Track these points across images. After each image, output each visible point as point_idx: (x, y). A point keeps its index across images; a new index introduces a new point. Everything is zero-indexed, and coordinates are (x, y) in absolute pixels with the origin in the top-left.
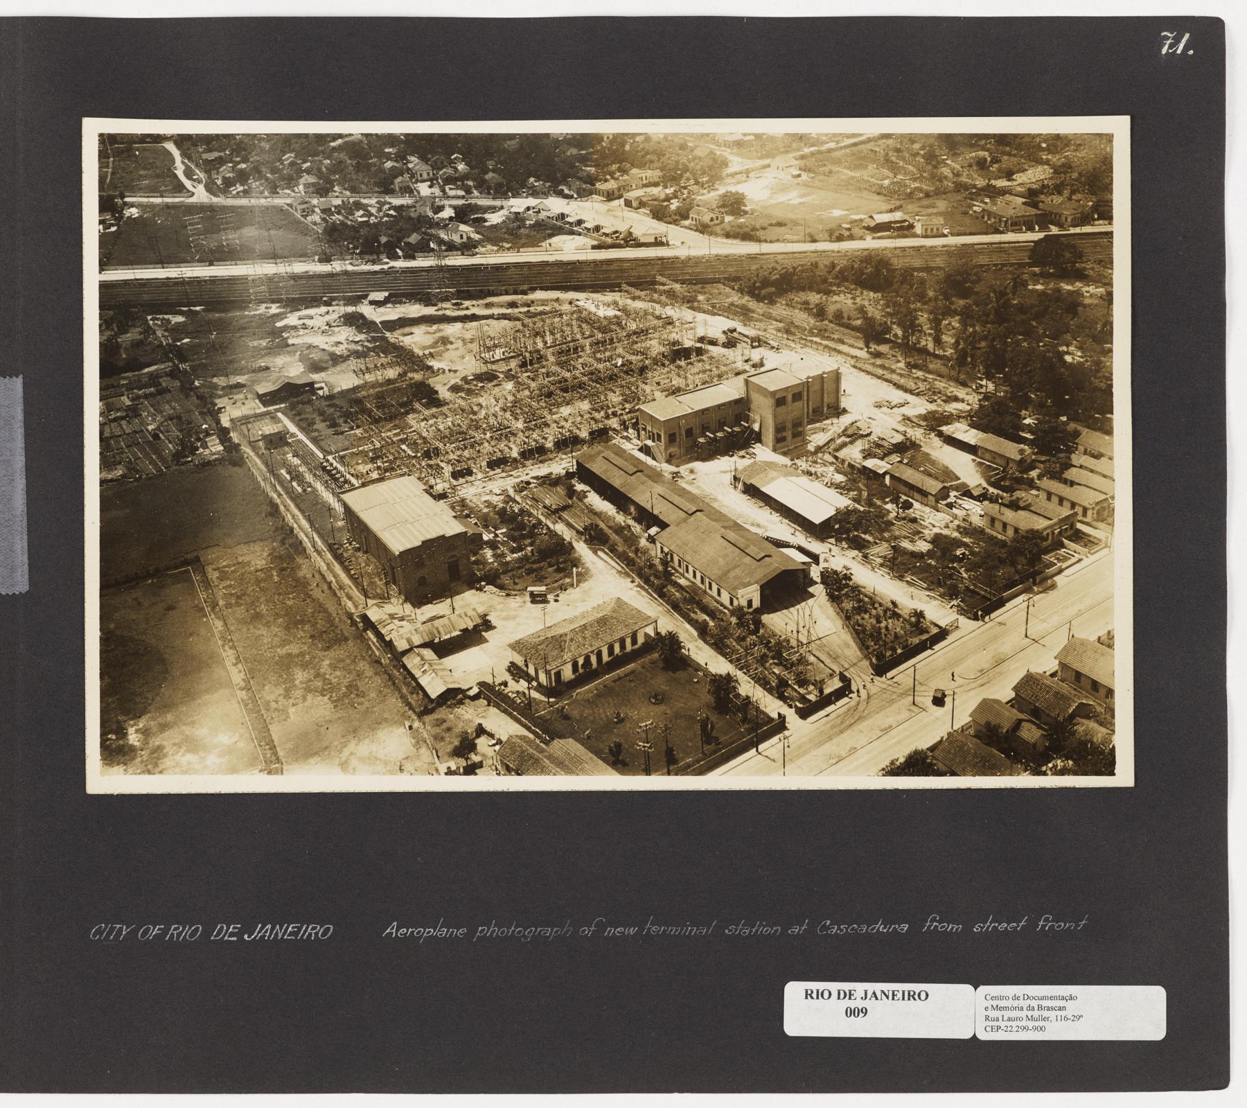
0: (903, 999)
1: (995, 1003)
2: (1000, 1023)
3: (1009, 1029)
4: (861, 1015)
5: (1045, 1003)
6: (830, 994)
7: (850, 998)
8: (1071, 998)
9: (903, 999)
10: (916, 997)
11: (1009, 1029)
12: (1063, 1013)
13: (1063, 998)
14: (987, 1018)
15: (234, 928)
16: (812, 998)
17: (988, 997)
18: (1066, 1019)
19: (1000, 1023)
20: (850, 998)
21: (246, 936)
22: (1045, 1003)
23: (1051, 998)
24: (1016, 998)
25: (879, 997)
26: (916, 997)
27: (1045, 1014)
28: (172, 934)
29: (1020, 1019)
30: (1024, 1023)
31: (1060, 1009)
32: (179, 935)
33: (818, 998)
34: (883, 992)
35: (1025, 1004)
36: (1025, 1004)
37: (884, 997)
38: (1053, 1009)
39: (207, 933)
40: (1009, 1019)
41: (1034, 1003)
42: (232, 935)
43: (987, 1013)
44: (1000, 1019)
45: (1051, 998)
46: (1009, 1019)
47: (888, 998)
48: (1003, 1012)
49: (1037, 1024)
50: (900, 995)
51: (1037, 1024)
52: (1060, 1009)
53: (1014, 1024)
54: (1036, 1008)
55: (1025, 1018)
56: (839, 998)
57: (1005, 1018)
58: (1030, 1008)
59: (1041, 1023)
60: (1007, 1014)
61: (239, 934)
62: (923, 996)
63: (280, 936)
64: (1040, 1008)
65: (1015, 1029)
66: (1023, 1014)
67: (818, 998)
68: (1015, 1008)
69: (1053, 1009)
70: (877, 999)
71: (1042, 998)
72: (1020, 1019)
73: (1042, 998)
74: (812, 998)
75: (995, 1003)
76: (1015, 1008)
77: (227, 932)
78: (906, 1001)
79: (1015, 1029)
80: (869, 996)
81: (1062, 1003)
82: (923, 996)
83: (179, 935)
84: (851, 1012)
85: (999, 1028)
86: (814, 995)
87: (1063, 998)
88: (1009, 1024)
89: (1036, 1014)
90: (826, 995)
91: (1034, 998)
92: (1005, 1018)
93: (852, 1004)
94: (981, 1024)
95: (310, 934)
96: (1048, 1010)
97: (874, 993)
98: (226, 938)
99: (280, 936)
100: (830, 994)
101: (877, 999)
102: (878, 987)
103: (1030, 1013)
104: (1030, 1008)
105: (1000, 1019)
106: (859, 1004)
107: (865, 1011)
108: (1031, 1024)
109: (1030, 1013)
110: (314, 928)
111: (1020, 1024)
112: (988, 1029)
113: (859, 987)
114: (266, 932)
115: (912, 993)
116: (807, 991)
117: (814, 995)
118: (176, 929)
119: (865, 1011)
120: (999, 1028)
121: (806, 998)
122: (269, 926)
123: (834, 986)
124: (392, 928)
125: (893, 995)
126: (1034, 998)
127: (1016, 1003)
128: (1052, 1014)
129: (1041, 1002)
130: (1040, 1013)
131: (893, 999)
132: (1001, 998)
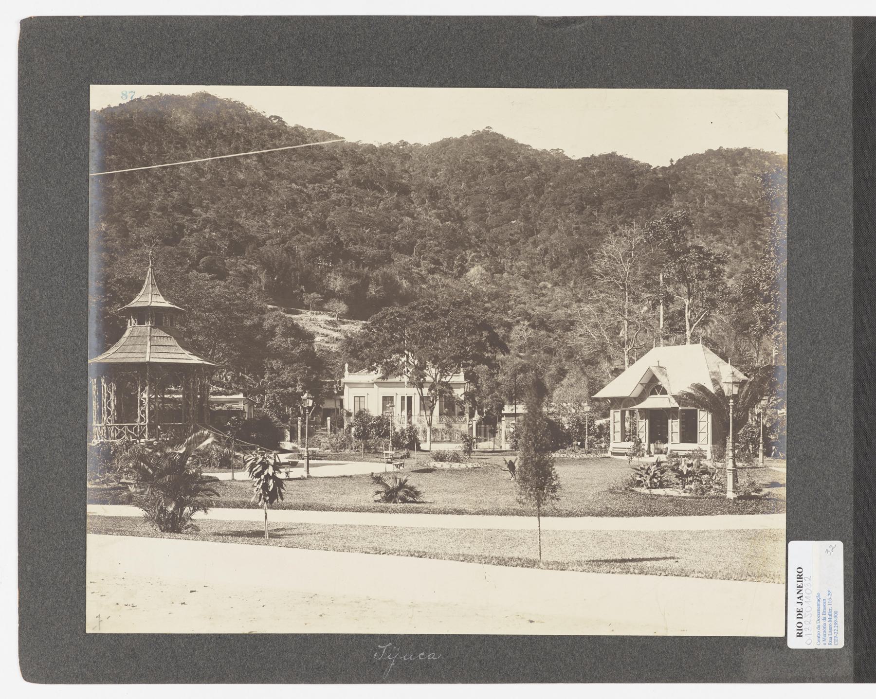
1: (822, 639)
2: (833, 637)
5: (822, 612)
8: (819, 596)
11: (836, 631)
12: (827, 601)
13: (819, 600)
14: (830, 644)
18: (830, 599)
19: (833, 637)
23: (819, 609)
24: (819, 628)
27: (827, 611)
29: (830, 625)
31: (824, 602)
35: (822, 622)
38: (825, 606)
40: (831, 631)
41: (822, 617)
44: (830, 636)
45: (819, 609)
46: (831, 631)
49: (833, 616)
51: (833, 616)
52: (824, 602)
55: (830, 622)
65: (836, 628)
66: (828, 624)
69: (825, 609)
72: (830, 625)
73: (819, 612)
75: (822, 639)
79: (836, 628)
85: (835, 637)
87: (819, 600)
88: (833, 632)
89: (827, 616)
96: (825, 609)
105: (831, 636)
108: (833, 619)
111: (833, 626)
120: (835, 637)
127: (822, 628)
128: (828, 607)
130: (827, 614)
132: (819, 636)
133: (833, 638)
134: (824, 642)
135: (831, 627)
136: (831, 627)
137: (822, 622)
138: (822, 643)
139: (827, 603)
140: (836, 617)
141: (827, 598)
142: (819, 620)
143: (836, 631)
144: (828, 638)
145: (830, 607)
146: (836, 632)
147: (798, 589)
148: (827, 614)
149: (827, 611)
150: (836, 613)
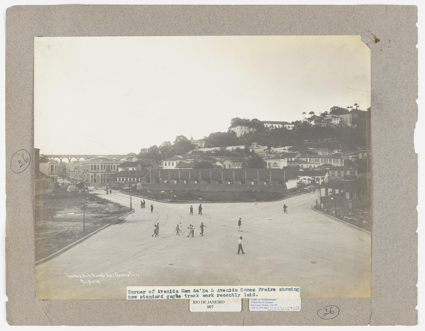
2: (255, 306)
3: (257, 308)
8: (275, 300)
12: (272, 304)
13: (272, 300)
14: (251, 305)
18: (273, 305)
19: (255, 306)
23: (269, 300)
24: (259, 300)
27: (267, 304)
30: (261, 306)
31: (271, 303)
35: (262, 301)
38: (269, 303)
40: (257, 305)
41: (264, 301)
43: (251, 304)
44: (255, 305)
45: (269, 300)
46: (257, 305)
49: (264, 306)
52: (271, 303)
53: (259, 307)
54: (265, 303)
55: (262, 305)
57: (256, 305)
58: (263, 302)
60: (257, 304)
64: (266, 302)
65: (259, 308)
66: (261, 304)
68: (259, 302)
69: (269, 303)
71: (267, 300)
73: (267, 300)
75: (254, 301)
76: (259, 302)
79: (259, 308)
85: (255, 308)
87: (272, 300)
88: (258, 306)
89: (265, 304)
92: (256, 305)
96: (268, 303)
103: (264, 304)
104: (263, 302)
105: (255, 305)
108: (263, 307)
109: (263, 304)
111: (260, 306)
112: (252, 308)
120: (255, 308)
127: (259, 301)
129: (266, 301)
130: (266, 304)
133: (254, 306)
135: (259, 305)
136: (259, 305)
137: (262, 301)
138: (252, 301)
139: (271, 304)
140: (264, 308)
141: (274, 304)
143: (257, 308)
144: (254, 304)
145: (269, 305)
146: (257, 308)
147: (215, 301)
148: (266, 304)
150: (266, 308)
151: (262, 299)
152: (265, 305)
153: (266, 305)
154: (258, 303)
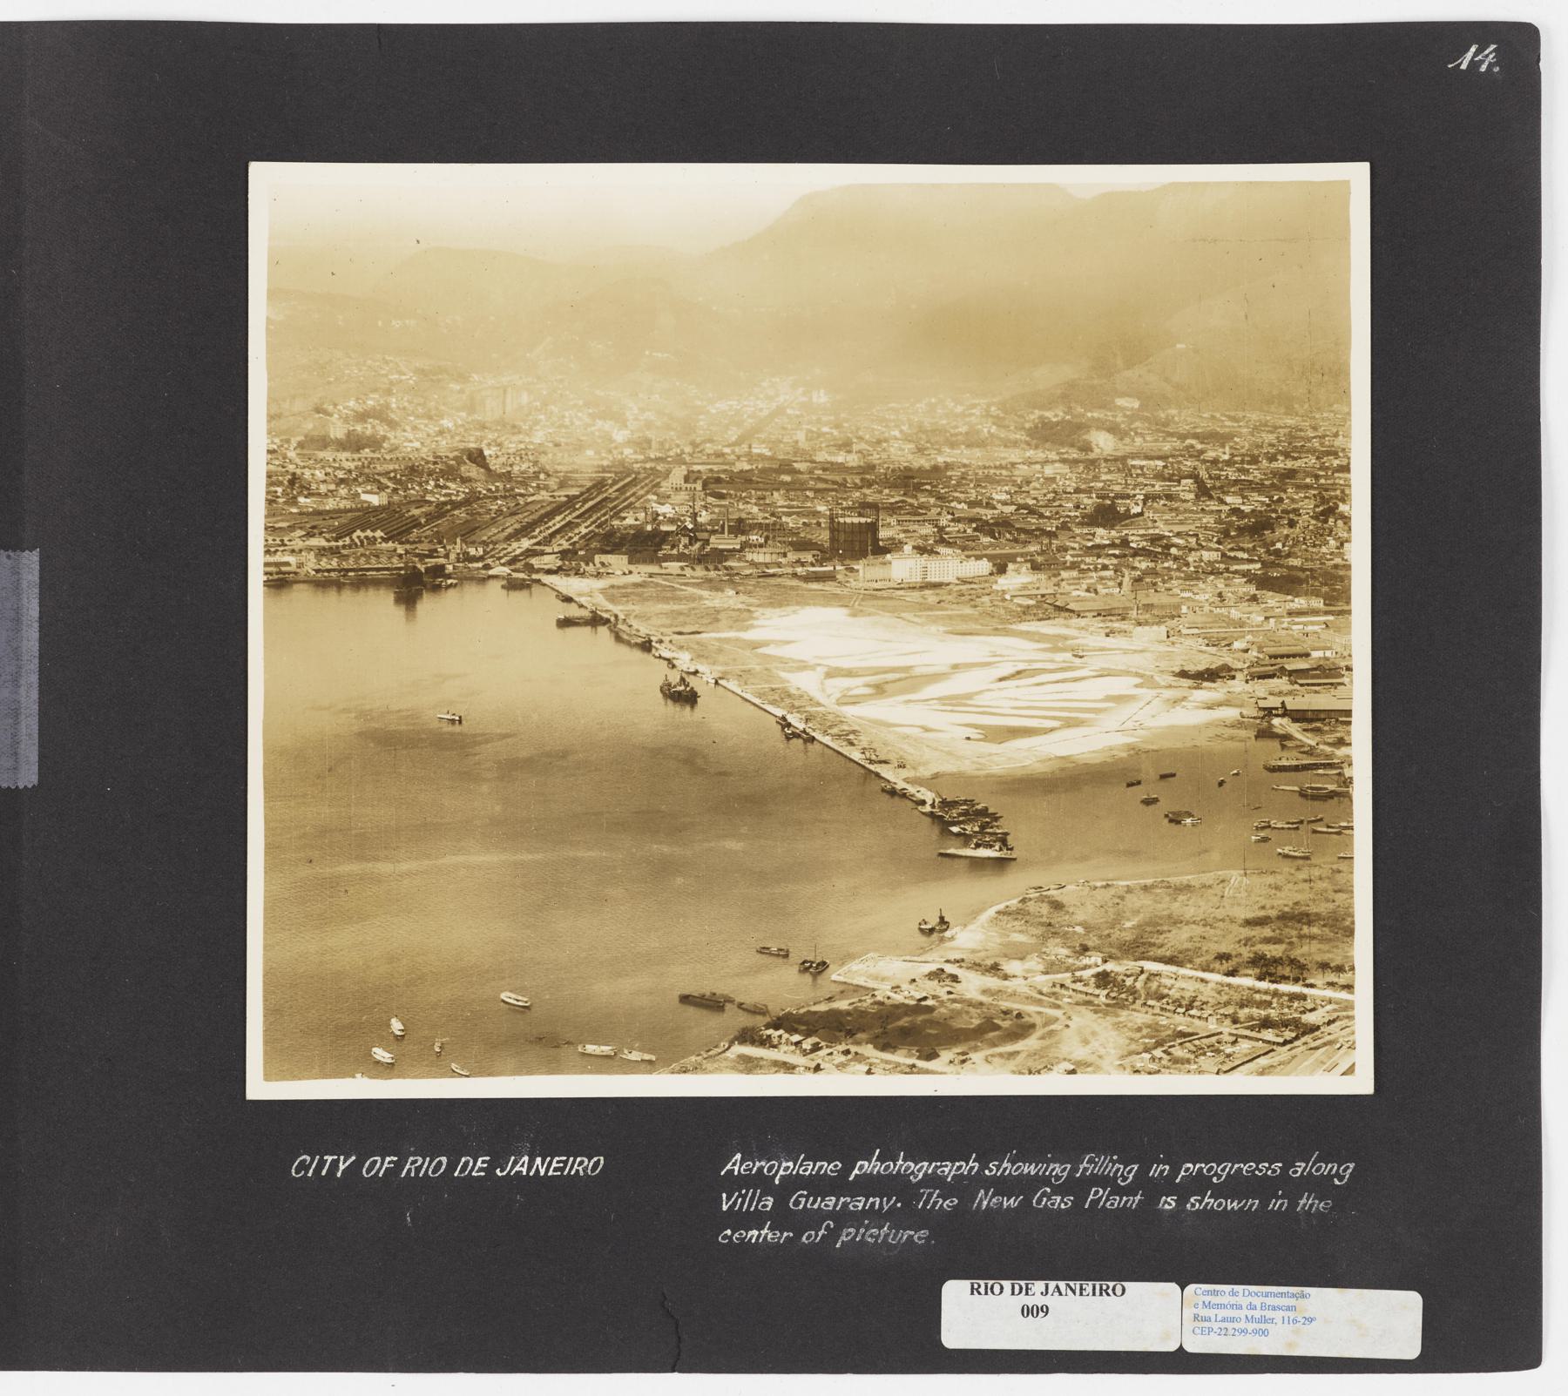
0: (1094, 1294)
1: (1207, 1299)
2: (1216, 1326)
3: (1223, 1332)
4: (1041, 1314)
5: (1270, 1301)
6: (1002, 1288)
7: (1027, 1294)
8: (1303, 1296)
9: (1094, 1294)
10: (1110, 1291)
12: (1292, 1315)
13: (1294, 1296)
15: (483, 1162)
16: (979, 1293)
17: (1199, 1292)
18: (1295, 1321)
19: (1216, 1326)
20: (1027, 1294)
21: (498, 1171)
22: (1270, 1301)
25: (1064, 1293)
26: (1110, 1291)
27: (1269, 1314)
28: (409, 1170)
30: (1242, 1325)
31: (1289, 1308)
32: (418, 1169)
33: (986, 1293)
34: (1068, 1285)
35: (1244, 1301)
36: (1244, 1301)
37: (1069, 1292)
38: (1280, 1308)
39: (452, 1166)
40: (1224, 1320)
41: (1257, 1301)
42: (481, 1170)
43: (1195, 1311)
44: (1213, 1319)
45: (1275, 1295)
46: (1224, 1320)
47: (1074, 1293)
48: (1216, 1311)
50: (1089, 1289)
52: (1289, 1308)
53: (1230, 1326)
54: (1259, 1307)
55: (1243, 1318)
56: (1013, 1294)
57: (1219, 1318)
58: (1252, 1307)
59: (1263, 1326)
60: (1222, 1313)
61: (490, 1170)
62: (1119, 1290)
63: (542, 1172)
66: (1242, 1314)
67: (986, 1293)
69: (1280, 1308)
70: (1061, 1294)
74: (979, 1293)
75: (1207, 1299)
77: (477, 1166)
78: (1098, 1297)
80: (1050, 1291)
81: (1292, 1302)
82: (1119, 1291)
83: (418, 1169)
84: (1027, 1311)
85: (1210, 1330)
86: (982, 1290)
89: (1257, 1314)
90: (997, 1289)
91: (1256, 1294)
92: (1219, 1318)
93: (1030, 1301)
94: (1189, 1325)
95: (577, 1171)
96: (1274, 1308)
97: (1057, 1287)
98: (474, 1174)
99: (542, 1172)
100: (1002, 1288)
101: (1061, 1294)
102: (1062, 1285)
104: (1252, 1307)
105: (1213, 1319)
106: (1036, 1300)
107: (1045, 1310)
108: (1251, 1327)
110: (581, 1163)
111: (1236, 1325)
112: (1197, 1331)
113: (1038, 1286)
114: (522, 1166)
115: (1104, 1287)
116: (972, 1286)
117: (982, 1290)
118: (414, 1162)
119: (1045, 1310)
121: (972, 1293)
122: (526, 1159)
123: (1007, 1284)
124: (734, 1164)
125: (1081, 1289)
126: (1256, 1294)
127: (1233, 1300)
128: (1278, 1315)
130: (1264, 1313)
131: (1081, 1294)
133: (1207, 1324)
134: (1200, 1306)
135: (1233, 1320)
136: (1233, 1320)
140: (1255, 1332)
142: (1250, 1294)
148: (1264, 1313)
149: (1269, 1314)
150: (1264, 1333)
151: (1247, 1293)
152: (1264, 1320)
153: (1264, 1320)
154: (1225, 1307)
